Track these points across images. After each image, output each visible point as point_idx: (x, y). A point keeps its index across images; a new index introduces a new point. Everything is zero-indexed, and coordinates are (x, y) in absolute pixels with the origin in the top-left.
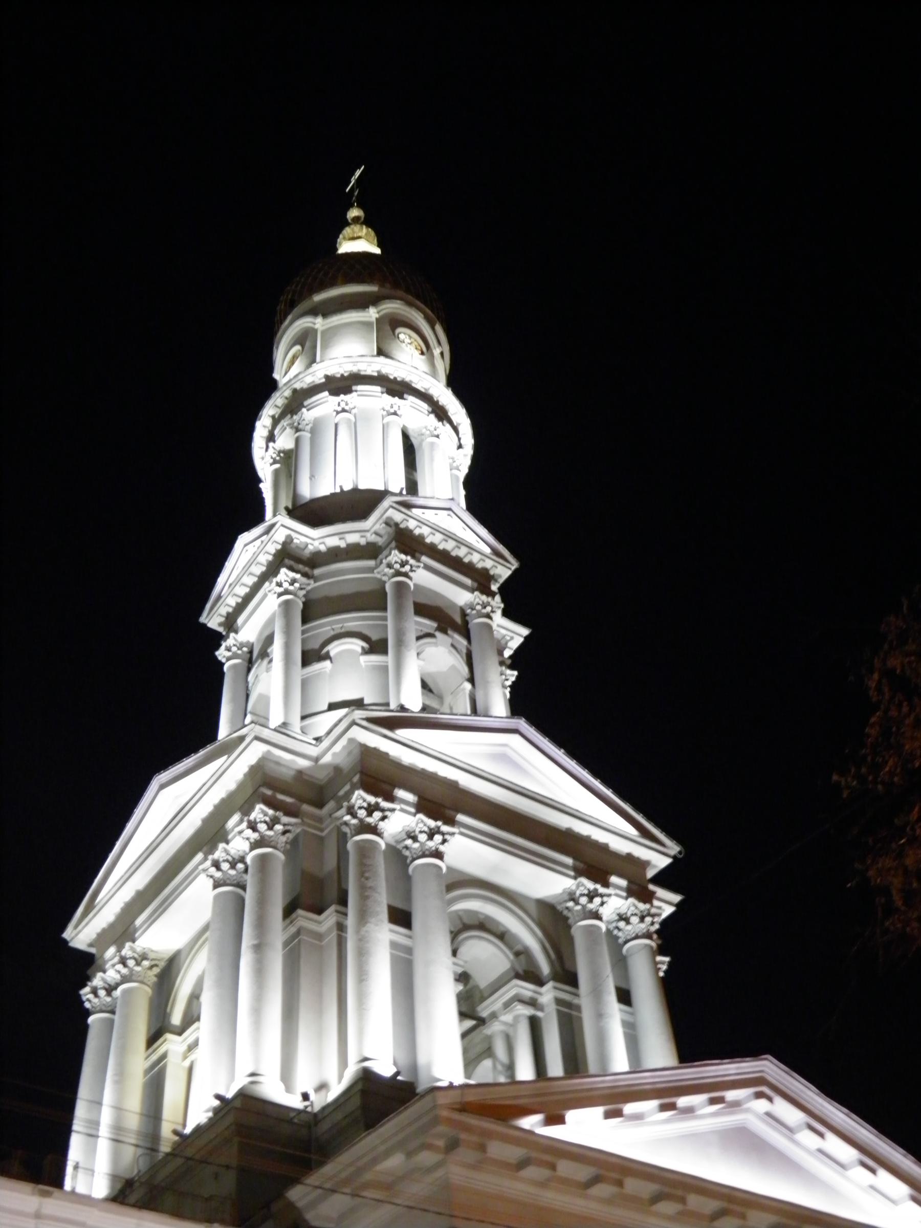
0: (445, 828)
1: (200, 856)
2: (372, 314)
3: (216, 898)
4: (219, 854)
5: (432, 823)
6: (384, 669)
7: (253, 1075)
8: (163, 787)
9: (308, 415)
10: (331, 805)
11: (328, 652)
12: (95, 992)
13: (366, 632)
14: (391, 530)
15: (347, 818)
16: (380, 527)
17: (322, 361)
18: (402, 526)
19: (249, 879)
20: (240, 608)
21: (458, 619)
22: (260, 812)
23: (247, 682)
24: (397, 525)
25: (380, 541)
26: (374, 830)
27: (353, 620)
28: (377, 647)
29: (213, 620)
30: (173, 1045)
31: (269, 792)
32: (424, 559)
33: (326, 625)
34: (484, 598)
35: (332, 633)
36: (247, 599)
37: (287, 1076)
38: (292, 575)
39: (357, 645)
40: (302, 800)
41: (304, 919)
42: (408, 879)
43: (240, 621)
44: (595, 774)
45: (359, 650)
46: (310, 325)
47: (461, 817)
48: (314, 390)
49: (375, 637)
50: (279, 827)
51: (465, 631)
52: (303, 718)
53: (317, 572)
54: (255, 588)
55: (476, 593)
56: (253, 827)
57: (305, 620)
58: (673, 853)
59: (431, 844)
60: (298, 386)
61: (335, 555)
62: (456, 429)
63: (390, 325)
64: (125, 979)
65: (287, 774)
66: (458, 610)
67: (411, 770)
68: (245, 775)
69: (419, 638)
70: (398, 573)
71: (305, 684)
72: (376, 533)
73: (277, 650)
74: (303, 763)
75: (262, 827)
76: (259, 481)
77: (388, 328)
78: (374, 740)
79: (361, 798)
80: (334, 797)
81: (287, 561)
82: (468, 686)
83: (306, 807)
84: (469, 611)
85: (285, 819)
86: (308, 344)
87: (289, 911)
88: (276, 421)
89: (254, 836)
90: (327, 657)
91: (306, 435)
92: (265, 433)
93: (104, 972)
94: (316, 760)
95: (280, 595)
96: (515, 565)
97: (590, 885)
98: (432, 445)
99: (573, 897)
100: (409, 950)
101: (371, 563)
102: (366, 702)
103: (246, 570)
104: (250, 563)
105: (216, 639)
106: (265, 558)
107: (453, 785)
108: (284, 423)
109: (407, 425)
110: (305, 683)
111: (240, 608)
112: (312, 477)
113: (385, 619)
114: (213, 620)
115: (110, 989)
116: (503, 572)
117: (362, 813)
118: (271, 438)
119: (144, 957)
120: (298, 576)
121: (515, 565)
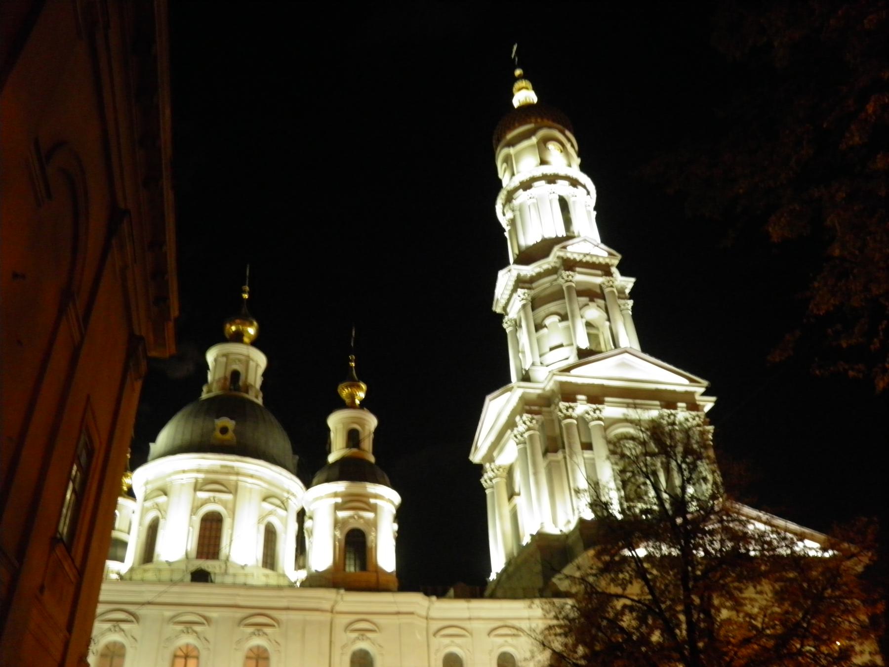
0: (600, 406)
1: (509, 431)
2: (534, 140)
3: (519, 450)
4: (515, 432)
5: (594, 406)
6: (568, 328)
8: (490, 400)
9: (516, 203)
10: (553, 407)
12: (486, 481)
14: (561, 260)
15: (560, 413)
16: (555, 260)
17: (518, 172)
19: (527, 442)
20: (507, 304)
21: (598, 291)
22: (526, 417)
23: (517, 337)
24: (562, 258)
25: (558, 265)
26: (570, 417)
27: (552, 307)
28: (564, 318)
29: (498, 309)
30: (516, 499)
31: (527, 408)
32: (578, 269)
33: (543, 310)
34: (608, 278)
36: (509, 300)
37: (555, 522)
38: (523, 291)
39: (556, 318)
40: (541, 406)
41: (551, 457)
42: (589, 429)
43: (508, 310)
45: (558, 321)
47: (607, 399)
48: (516, 189)
49: (562, 312)
50: (534, 422)
51: (602, 296)
52: (541, 356)
53: (534, 285)
54: (511, 296)
55: (604, 277)
56: (524, 423)
57: (533, 309)
59: (595, 416)
60: (509, 188)
61: (540, 276)
62: (584, 187)
63: (543, 143)
65: (534, 397)
66: (598, 287)
67: (583, 385)
68: (519, 400)
69: (581, 309)
70: (567, 281)
71: (538, 341)
72: (555, 262)
73: (524, 324)
74: (539, 391)
75: (528, 423)
76: (504, 230)
77: (543, 145)
78: (564, 378)
79: (563, 405)
81: (520, 285)
82: (607, 323)
83: (545, 409)
84: (602, 285)
85: (536, 417)
86: (509, 163)
87: (545, 453)
88: (504, 206)
89: (526, 427)
90: (545, 326)
91: (518, 213)
92: (501, 211)
93: (487, 472)
94: (544, 389)
95: (520, 301)
96: (619, 256)
97: (668, 411)
98: (574, 202)
100: (593, 459)
101: (555, 277)
102: (564, 344)
103: (505, 289)
104: (507, 284)
105: (501, 317)
106: (511, 284)
107: (602, 386)
108: (507, 208)
109: (561, 194)
110: (538, 341)
111: (507, 304)
112: (524, 234)
113: (565, 303)
114: (498, 309)
115: (491, 480)
116: (616, 262)
117: (565, 411)
118: (504, 215)
119: (500, 467)
120: (526, 291)
121: (619, 256)
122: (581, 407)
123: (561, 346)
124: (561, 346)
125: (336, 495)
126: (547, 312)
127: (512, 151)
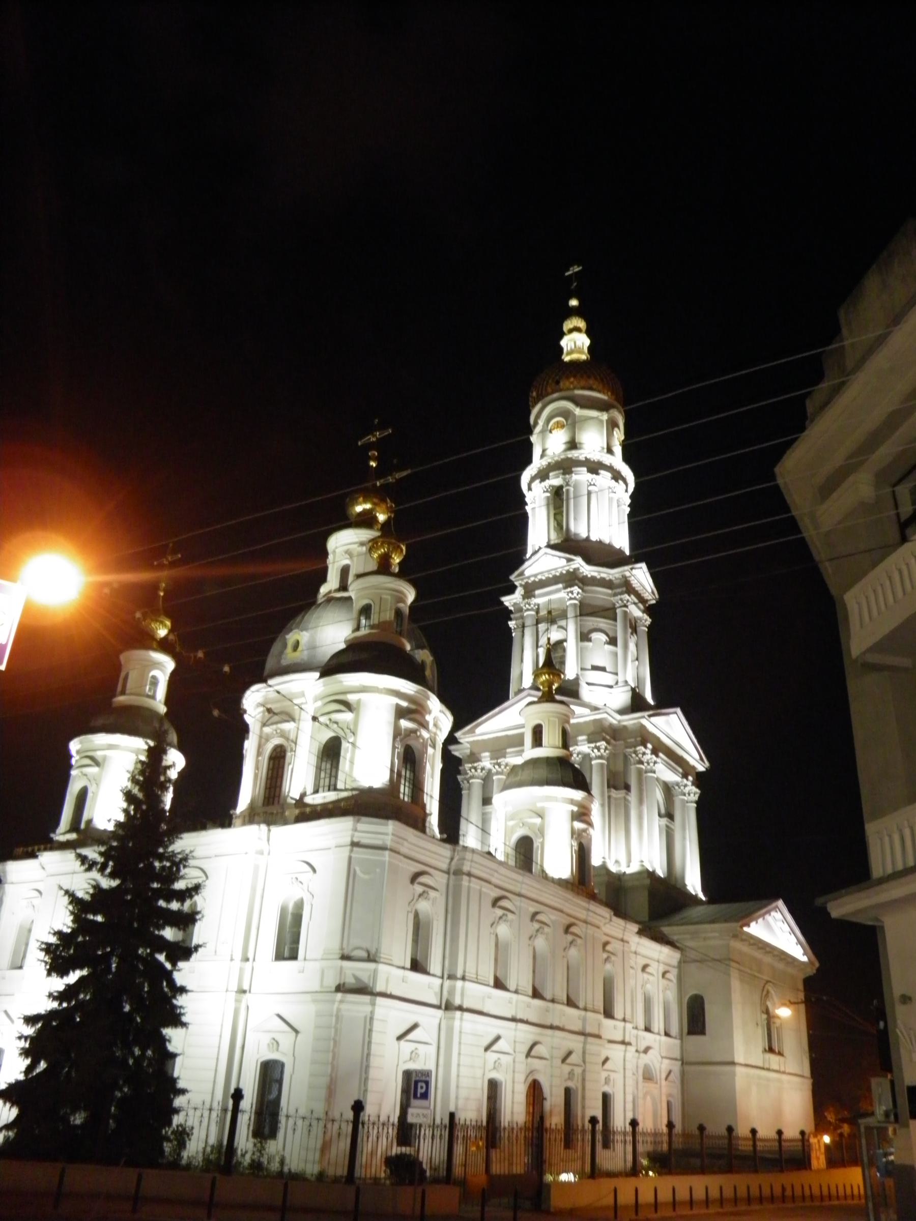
2: (605, 416)
7: (604, 858)
11: (591, 638)
13: (608, 631)
14: (623, 580)
18: (628, 579)
25: (615, 582)
27: (602, 623)
28: (613, 641)
35: (592, 627)
39: (604, 638)
44: (694, 733)
45: (605, 640)
46: (572, 409)
47: (661, 755)
48: (579, 463)
49: (611, 634)
53: (587, 588)
58: (706, 766)
61: (594, 581)
64: (498, 773)
74: (615, 722)
80: (625, 740)
83: (612, 741)
99: (678, 784)
112: (575, 519)
113: (616, 626)
120: (580, 591)
122: (649, 756)
123: (603, 669)
124: (603, 669)
125: (572, 802)
126: (595, 626)
127: (578, 411)
